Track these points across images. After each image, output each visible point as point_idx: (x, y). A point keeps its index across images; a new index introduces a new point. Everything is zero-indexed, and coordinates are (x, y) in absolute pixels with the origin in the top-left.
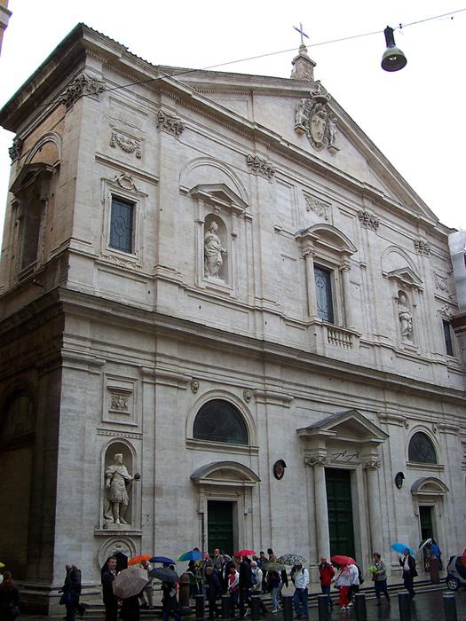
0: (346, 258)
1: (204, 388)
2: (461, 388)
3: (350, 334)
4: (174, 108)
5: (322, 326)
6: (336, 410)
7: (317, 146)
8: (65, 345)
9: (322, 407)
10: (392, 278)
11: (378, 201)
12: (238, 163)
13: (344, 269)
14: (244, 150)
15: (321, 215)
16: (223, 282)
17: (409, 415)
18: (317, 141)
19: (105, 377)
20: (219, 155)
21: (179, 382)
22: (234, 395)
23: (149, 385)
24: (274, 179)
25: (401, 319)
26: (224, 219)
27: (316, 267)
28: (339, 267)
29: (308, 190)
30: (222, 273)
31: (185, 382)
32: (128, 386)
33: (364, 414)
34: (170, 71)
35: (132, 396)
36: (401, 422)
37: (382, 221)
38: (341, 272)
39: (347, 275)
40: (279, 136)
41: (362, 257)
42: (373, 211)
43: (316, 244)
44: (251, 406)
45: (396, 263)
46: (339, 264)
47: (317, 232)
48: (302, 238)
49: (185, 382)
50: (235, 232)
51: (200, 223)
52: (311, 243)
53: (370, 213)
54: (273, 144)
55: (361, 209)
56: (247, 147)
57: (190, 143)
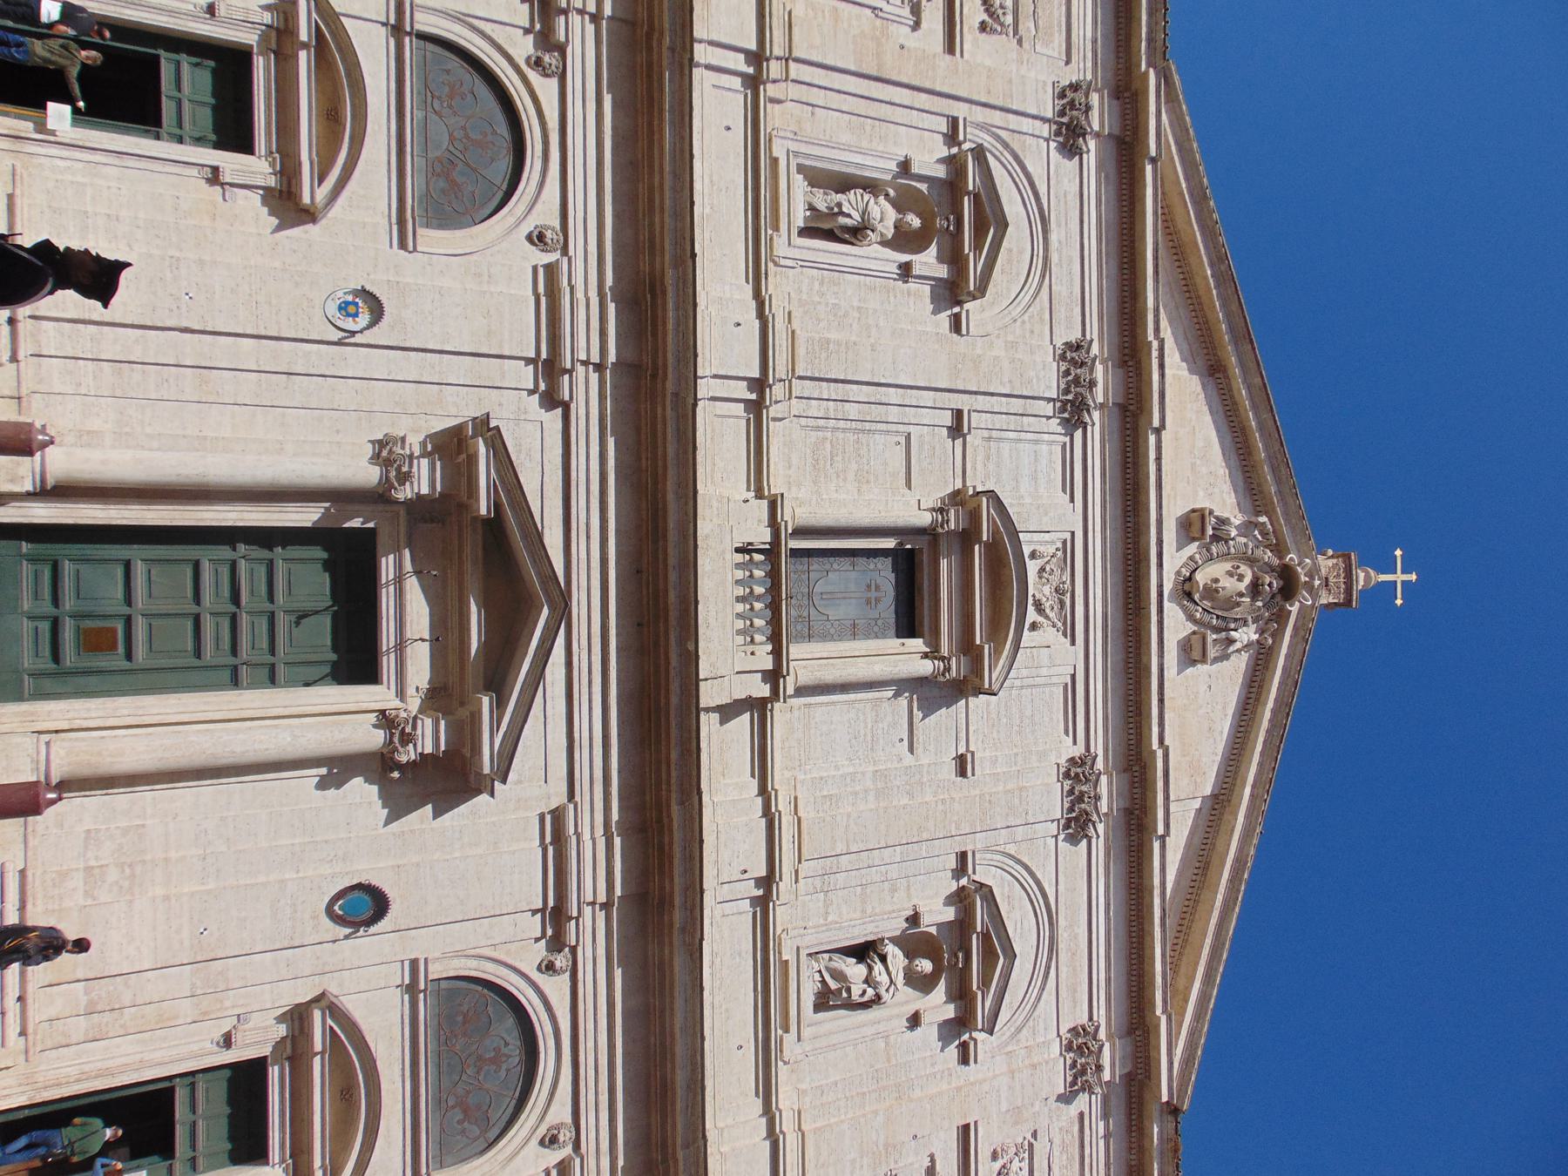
1: (547, 89)
2: (747, 716)
12: (1061, 312)
18: (1199, 576)
20: (1059, 251)
22: (541, 184)
30: (821, 228)
57: (1056, 171)
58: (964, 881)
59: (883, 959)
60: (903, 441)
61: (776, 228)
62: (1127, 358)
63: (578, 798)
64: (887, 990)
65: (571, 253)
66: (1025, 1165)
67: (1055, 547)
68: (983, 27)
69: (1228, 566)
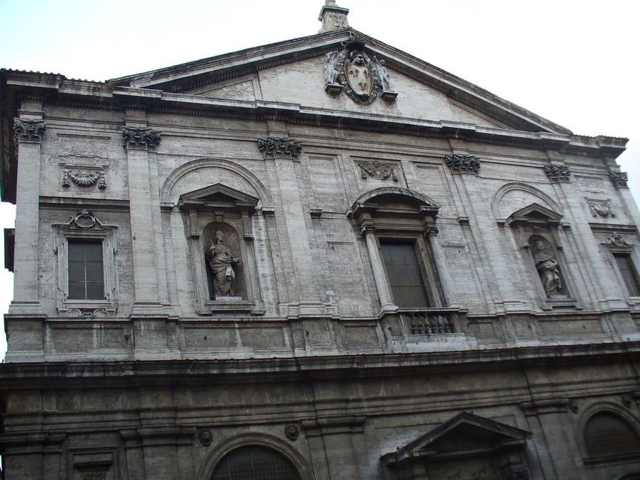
0: (429, 219)
1: (218, 437)
3: (448, 315)
4: (144, 119)
5: (397, 315)
6: (445, 417)
7: (362, 100)
8: (6, 429)
9: (419, 419)
10: (515, 223)
11: (469, 136)
13: (428, 234)
14: (252, 135)
15: (385, 178)
16: (241, 298)
17: (573, 394)
18: (361, 93)
19: (71, 455)
21: (179, 437)
23: (134, 451)
24: (304, 158)
25: (542, 272)
26: (233, 223)
27: (383, 243)
28: (422, 232)
29: (360, 154)
31: (191, 436)
32: (108, 457)
33: (476, 413)
34: (125, 82)
35: (111, 469)
36: (561, 406)
37: (482, 157)
38: (427, 240)
39: (436, 242)
40: (296, 105)
41: (461, 209)
42: (467, 150)
43: (374, 214)
44: (300, 444)
45: (521, 201)
46: (421, 229)
47: (371, 200)
48: (355, 216)
49: (191, 436)
50: (247, 235)
51: (196, 238)
52: (366, 216)
53: (463, 153)
54: (291, 117)
55: (449, 153)
56: (258, 131)
58: (507, 225)
59: (541, 263)
60: (331, 245)
61: (248, 312)
62: (262, 119)
63: (519, 401)
64: (553, 262)
65: (299, 419)
66: (598, 203)
67: (359, 167)
68: (103, 188)
69: (351, 77)
